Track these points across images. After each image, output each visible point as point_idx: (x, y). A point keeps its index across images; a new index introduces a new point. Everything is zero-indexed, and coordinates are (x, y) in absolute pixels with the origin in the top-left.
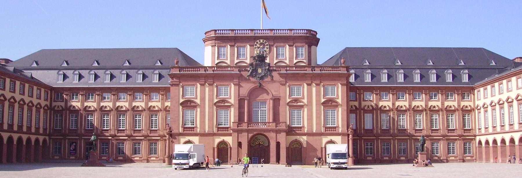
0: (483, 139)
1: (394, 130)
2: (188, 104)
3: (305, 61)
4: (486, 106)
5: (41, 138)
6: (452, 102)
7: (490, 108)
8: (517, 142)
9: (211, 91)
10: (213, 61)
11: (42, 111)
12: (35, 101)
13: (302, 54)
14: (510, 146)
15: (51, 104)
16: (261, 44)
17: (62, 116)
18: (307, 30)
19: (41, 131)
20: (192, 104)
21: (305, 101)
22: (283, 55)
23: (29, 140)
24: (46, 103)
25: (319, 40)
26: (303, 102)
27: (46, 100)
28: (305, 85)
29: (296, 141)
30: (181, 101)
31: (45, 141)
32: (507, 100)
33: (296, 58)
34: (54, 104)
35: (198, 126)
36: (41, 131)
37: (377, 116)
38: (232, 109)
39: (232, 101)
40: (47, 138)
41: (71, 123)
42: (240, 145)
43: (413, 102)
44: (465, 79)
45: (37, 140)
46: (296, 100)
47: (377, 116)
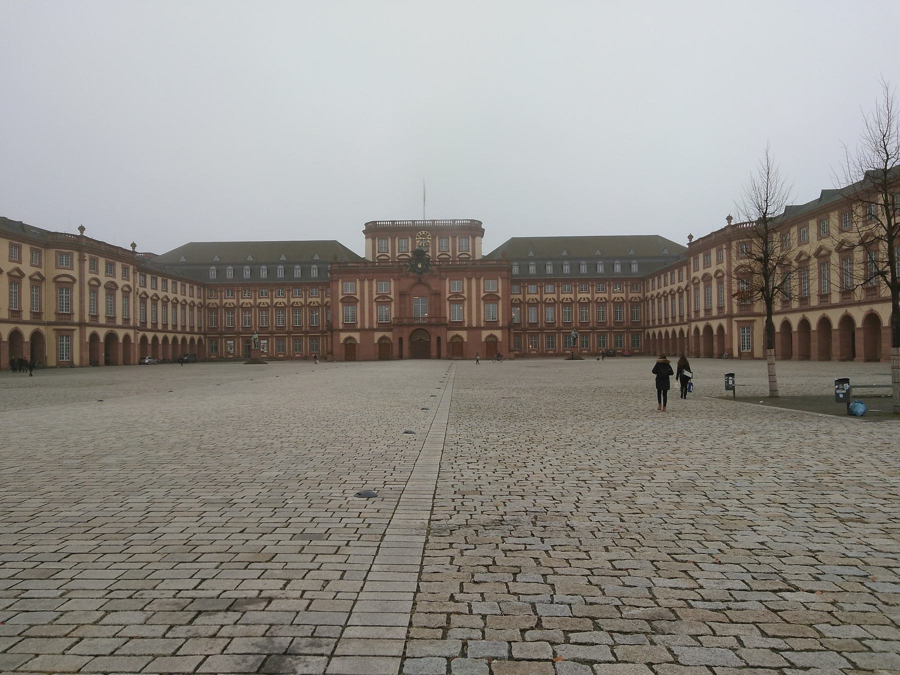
0: (651, 331)
1: (559, 323)
2: (349, 301)
5: (196, 337)
7: (656, 300)
9: (370, 287)
10: (374, 254)
11: (196, 309)
12: (189, 300)
15: (204, 301)
16: (423, 236)
17: (216, 313)
19: (196, 330)
20: (353, 300)
21: (465, 295)
23: (184, 340)
24: (199, 300)
27: (199, 297)
29: (457, 336)
30: (341, 297)
31: (200, 340)
32: (678, 291)
34: (208, 301)
35: (359, 322)
36: (196, 330)
37: (542, 310)
38: (393, 304)
39: (392, 296)
40: (202, 336)
41: (226, 320)
42: (401, 339)
45: (192, 340)
46: (457, 295)
47: (542, 310)
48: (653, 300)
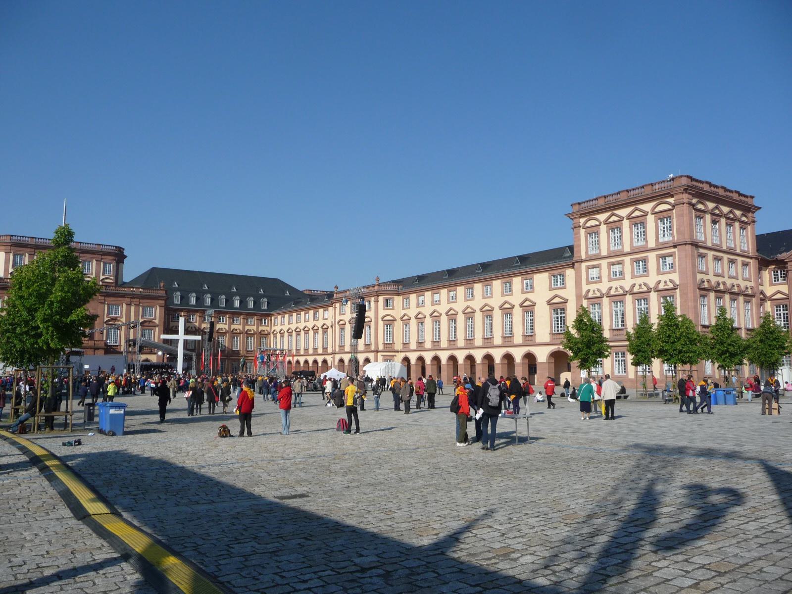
3: (112, 278)
4: (282, 332)
6: (252, 326)
7: (286, 334)
8: (346, 363)
13: (109, 271)
14: (322, 366)
18: (116, 247)
21: (123, 320)
22: (89, 269)
25: (126, 257)
26: (120, 321)
28: (124, 305)
33: (103, 274)
43: (232, 326)
44: (264, 306)
46: (115, 319)
48: (282, 335)
